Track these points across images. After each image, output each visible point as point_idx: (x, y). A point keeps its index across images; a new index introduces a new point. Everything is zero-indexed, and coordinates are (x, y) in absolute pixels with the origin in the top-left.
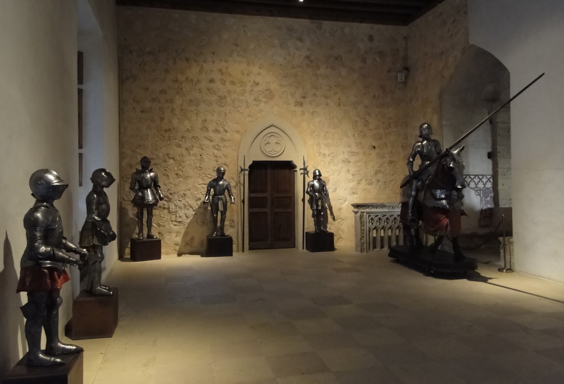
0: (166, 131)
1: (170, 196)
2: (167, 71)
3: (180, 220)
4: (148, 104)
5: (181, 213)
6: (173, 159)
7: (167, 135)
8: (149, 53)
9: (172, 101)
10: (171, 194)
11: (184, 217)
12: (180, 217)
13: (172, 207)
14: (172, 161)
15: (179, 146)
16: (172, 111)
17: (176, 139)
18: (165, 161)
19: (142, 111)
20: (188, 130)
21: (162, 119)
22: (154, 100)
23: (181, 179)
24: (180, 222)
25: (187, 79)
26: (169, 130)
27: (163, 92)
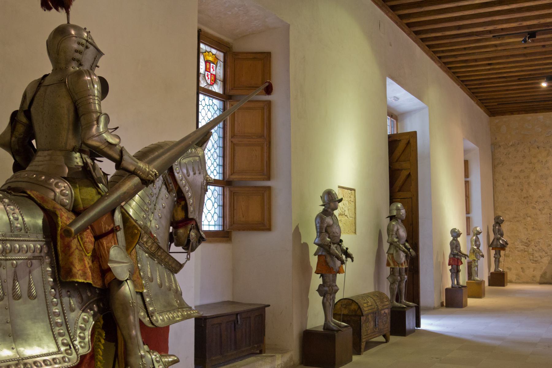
0: (524, 198)
1: (529, 243)
2: (524, 157)
3: (537, 259)
4: (512, 181)
5: (537, 255)
6: (530, 217)
7: (525, 200)
8: (511, 146)
9: (528, 177)
10: (529, 241)
11: (539, 258)
12: (536, 257)
13: (531, 250)
14: (529, 218)
15: (534, 208)
16: (529, 184)
17: (531, 203)
18: (524, 219)
19: (508, 186)
20: (540, 197)
21: (522, 190)
22: (516, 177)
23: (536, 231)
24: (536, 261)
25: (538, 161)
26: (527, 197)
27: (522, 171)
